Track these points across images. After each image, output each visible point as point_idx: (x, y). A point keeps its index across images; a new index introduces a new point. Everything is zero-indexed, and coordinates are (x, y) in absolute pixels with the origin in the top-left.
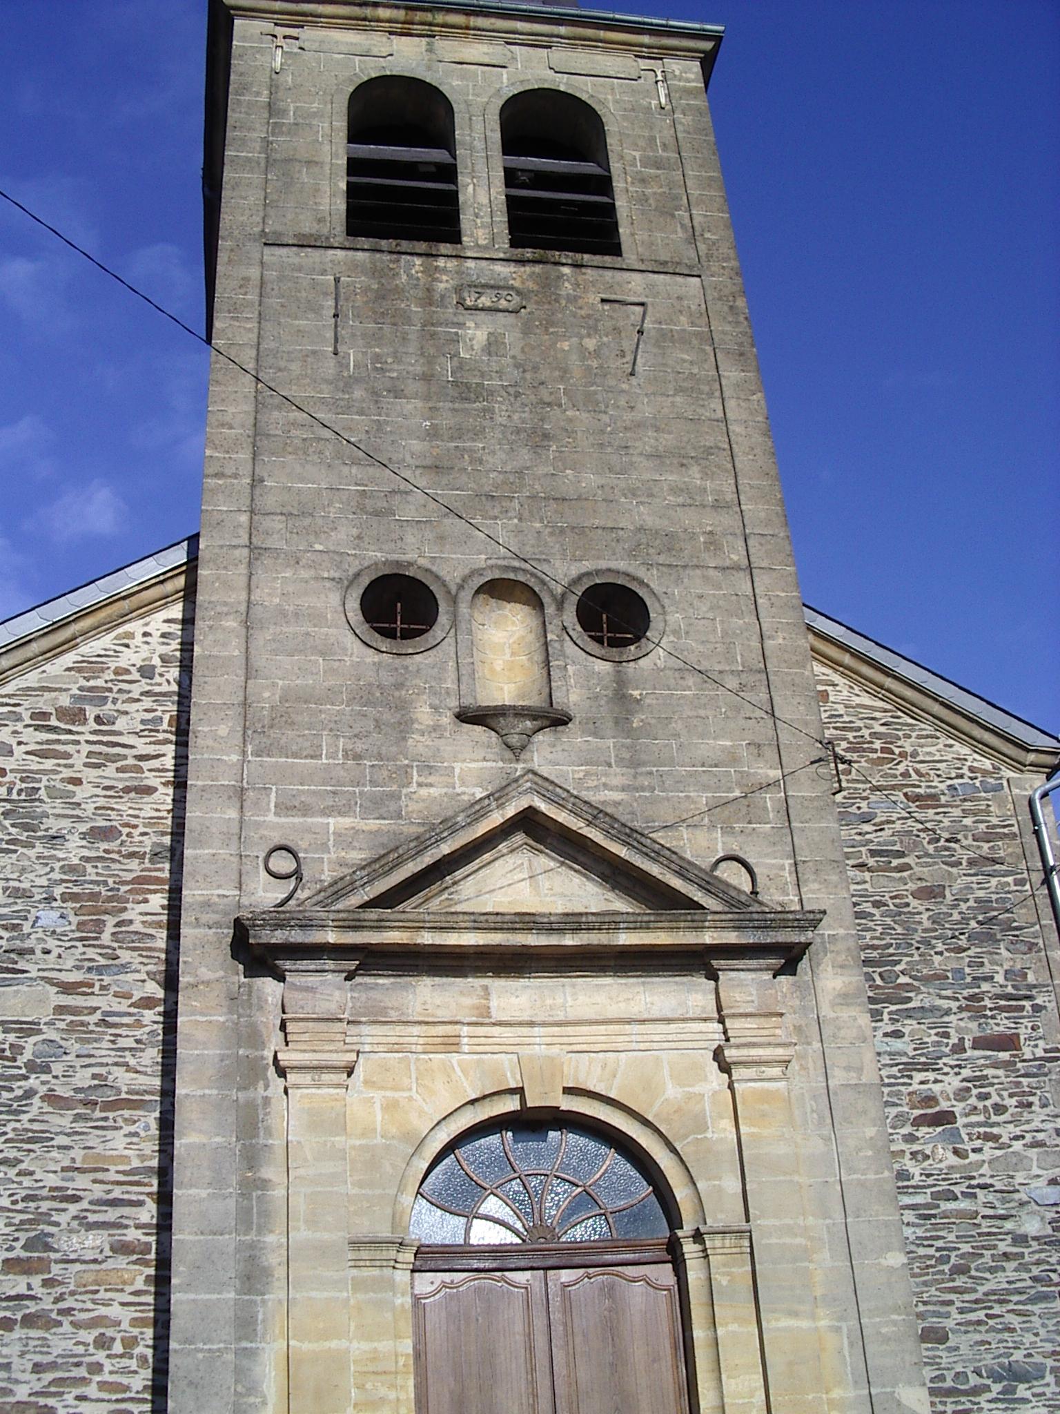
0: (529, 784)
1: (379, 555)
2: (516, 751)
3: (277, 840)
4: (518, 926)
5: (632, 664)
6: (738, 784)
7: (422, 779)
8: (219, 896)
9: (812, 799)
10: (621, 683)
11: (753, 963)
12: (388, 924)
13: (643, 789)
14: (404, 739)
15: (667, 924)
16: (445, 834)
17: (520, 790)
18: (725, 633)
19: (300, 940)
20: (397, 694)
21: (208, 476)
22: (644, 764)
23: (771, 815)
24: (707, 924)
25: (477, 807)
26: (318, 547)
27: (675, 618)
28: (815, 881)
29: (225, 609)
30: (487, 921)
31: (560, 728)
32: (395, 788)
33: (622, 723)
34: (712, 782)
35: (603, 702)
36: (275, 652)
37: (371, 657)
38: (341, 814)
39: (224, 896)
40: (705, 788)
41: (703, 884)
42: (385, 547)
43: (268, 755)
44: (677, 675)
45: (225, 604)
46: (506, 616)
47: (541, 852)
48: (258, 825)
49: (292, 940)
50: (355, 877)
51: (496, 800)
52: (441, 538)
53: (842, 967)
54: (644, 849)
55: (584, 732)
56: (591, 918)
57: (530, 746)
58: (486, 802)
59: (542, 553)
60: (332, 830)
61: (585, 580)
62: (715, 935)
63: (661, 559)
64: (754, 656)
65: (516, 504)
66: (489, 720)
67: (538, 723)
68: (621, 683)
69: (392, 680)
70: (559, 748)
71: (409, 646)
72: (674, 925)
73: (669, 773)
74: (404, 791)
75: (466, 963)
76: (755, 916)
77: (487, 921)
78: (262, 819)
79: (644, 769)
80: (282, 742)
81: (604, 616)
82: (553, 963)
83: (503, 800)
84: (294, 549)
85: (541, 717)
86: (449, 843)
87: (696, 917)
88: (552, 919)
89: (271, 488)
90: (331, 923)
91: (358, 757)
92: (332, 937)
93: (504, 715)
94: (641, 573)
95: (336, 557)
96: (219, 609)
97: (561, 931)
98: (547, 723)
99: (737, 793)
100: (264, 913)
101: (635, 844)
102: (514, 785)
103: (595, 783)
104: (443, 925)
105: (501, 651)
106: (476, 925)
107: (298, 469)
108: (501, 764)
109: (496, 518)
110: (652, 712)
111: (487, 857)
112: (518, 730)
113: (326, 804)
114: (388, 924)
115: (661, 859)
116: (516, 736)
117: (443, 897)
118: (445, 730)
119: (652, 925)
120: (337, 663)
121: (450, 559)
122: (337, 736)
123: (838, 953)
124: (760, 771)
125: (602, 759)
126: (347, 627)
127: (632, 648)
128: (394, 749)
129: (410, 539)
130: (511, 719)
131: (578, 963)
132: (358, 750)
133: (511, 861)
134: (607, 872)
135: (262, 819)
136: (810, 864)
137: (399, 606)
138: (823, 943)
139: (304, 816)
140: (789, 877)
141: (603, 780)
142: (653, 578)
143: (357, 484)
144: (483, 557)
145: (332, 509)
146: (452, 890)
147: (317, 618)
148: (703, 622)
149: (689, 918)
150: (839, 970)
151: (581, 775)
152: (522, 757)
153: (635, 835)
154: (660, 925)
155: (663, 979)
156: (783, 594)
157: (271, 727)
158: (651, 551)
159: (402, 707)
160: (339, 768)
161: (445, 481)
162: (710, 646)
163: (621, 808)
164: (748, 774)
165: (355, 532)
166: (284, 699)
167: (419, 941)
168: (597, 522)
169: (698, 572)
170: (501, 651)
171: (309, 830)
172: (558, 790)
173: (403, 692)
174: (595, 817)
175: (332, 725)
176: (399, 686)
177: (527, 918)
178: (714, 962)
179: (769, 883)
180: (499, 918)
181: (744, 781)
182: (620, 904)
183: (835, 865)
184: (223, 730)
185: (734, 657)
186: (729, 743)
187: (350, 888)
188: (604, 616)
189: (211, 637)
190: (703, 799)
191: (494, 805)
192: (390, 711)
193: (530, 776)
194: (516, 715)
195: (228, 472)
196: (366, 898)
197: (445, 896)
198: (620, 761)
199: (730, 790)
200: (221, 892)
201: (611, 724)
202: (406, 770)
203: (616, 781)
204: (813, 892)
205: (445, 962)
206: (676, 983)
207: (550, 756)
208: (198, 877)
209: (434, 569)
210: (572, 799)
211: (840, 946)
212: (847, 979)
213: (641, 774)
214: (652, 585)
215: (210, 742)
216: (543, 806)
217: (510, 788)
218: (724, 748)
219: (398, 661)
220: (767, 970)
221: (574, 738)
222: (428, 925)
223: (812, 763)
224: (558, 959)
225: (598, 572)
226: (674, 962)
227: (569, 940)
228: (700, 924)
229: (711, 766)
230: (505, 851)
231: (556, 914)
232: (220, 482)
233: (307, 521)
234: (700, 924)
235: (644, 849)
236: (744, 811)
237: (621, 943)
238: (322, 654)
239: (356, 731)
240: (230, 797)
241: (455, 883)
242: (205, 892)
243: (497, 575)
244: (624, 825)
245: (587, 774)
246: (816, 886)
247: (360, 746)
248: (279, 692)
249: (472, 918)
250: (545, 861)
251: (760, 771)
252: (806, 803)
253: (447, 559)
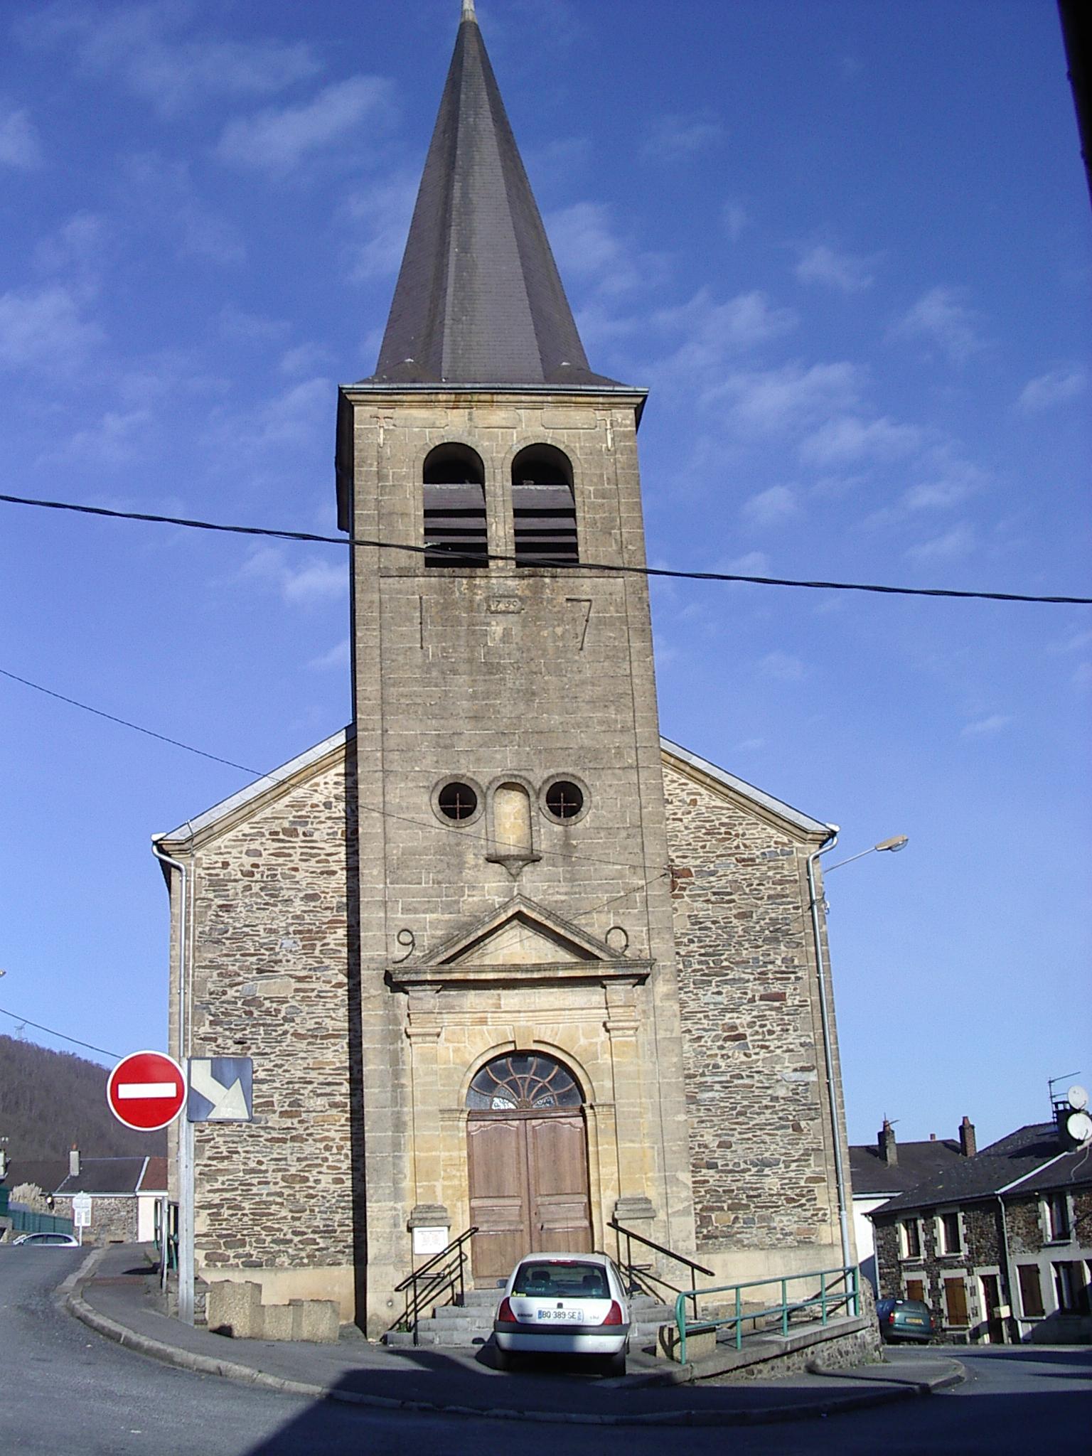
2: (515, 877)
3: (403, 927)
10: (567, 836)
33: (567, 857)
36: (398, 829)
40: (607, 892)
52: (478, 760)
63: (591, 765)
68: (567, 836)
71: (463, 822)
91: (439, 883)
92: (429, 977)
105: (508, 818)
121: (480, 773)
133: (512, 933)
137: (458, 801)
140: (645, 936)
142: (586, 777)
147: (417, 809)
159: (460, 855)
168: (558, 745)
170: (508, 818)
171: (417, 920)
176: (458, 844)
184: (375, 872)
192: (453, 859)
211: (668, 970)
216: (525, 910)
221: (543, 868)
233: (411, 754)
243: (507, 780)
247: (440, 877)
250: (527, 933)
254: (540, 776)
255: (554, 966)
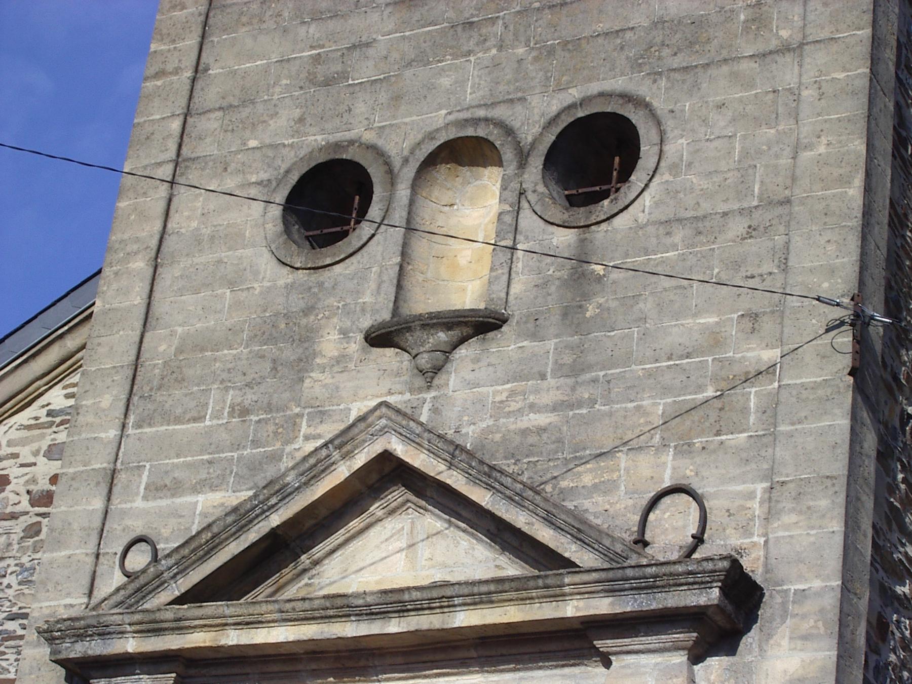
0: (383, 422)
1: (319, 138)
2: (431, 374)
3: (138, 532)
4: (331, 612)
5: (604, 226)
6: (715, 379)
7: (311, 431)
8: (65, 606)
9: (815, 386)
10: (581, 259)
11: (652, 641)
12: (187, 623)
13: (580, 404)
14: (301, 380)
15: (513, 595)
16: (273, 501)
17: (371, 430)
18: (745, 154)
19: (98, 652)
20: (304, 321)
21: (146, 79)
22: (590, 368)
23: (752, 419)
24: (567, 589)
25: (312, 461)
26: (253, 143)
27: (678, 146)
28: (793, 510)
29: (135, 247)
30: (294, 609)
31: (491, 335)
32: (278, 445)
33: (572, 315)
34: (677, 381)
35: (553, 289)
36: (181, 292)
37: (285, 277)
38: (213, 488)
39: (72, 606)
40: (666, 390)
41: (574, 532)
42: (329, 126)
43: (150, 425)
44: (662, 230)
45: (137, 240)
46: (485, 187)
47: (426, 510)
48: (124, 513)
49: (90, 652)
50: (161, 568)
51: (340, 447)
52: (397, 98)
53: (805, 638)
54: (508, 492)
55: (520, 336)
56: (416, 595)
57: (448, 365)
58: (324, 452)
59: (518, 89)
60: (199, 508)
61: (563, 117)
62: (581, 604)
63: (676, 62)
64: (780, 180)
65: (499, 28)
66: (396, 339)
67: (455, 334)
68: (581, 259)
69: (302, 304)
70: (484, 363)
71: (327, 255)
72: (524, 594)
73: (621, 377)
74: (288, 449)
75: (300, 667)
76: (630, 573)
77: (294, 609)
78: (128, 505)
79: (588, 376)
80: (167, 406)
81: (617, 159)
82: (400, 660)
83: (348, 447)
84: (224, 152)
85: (459, 324)
86: (280, 512)
87: (549, 581)
88: (369, 599)
89: (216, 76)
90: (129, 628)
91: (245, 412)
92: (131, 645)
93: (409, 329)
94: (643, 89)
95: (270, 153)
96: (129, 249)
97: (383, 615)
98: (466, 331)
99: (710, 392)
100: (58, 622)
101: (497, 485)
102: (362, 426)
103: (519, 405)
104: (248, 619)
105: (469, 238)
106: (284, 616)
107: (249, 42)
108: (408, 396)
109: (469, 53)
110: (615, 292)
111: (355, 524)
112: (427, 347)
113: (198, 477)
114: (187, 623)
115: (527, 503)
116: (425, 356)
117: (303, 582)
118: (351, 359)
119: (495, 597)
120: (245, 294)
121: (393, 129)
122: (227, 389)
123: (804, 617)
124: (749, 354)
125: (535, 370)
126: (535, 217)
127: (606, 202)
128: (286, 395)
129: (360, 108)
130: (418, 333)
131: (431, 657)
132: (246, 403)
133: (390, 525)
134: (493, 528)
135: (128, 505)
136: (792, 486)
137: (328, 202)
138: (784, 604)
139: (173, 496)
140: (756, 507)
141: (532, 398)
142: (658, 95)
143: (312, 47)
144: (444, 112)
145: (278, 89)
146: (314, 572)
147: (233, 238)
148: (716, 143)
149: (540, 582)
150: (799, 643)
151: (503, 397)
152: (436, 382)
153: (495, 474)
154: (505, 596)
155: (549, 672)
156: (841, 76)
157: (159, 389)
158: (666, 52)
159: (306, 339)
160: (222, 429)
161: (417, 16)
162: (717, 179)
163: (545, 436)
164: (731, 361)
165: (297, 113)
166: (180, 351)
167: (222, 643)
168: (600, 27)
169: (725, 69)
170: (469, 238)
171: (175, 513)
172: (412, 424)
173: (312, 318)
174: (453, 456)
175: (225, 375)
176: (308, 311)
177: (339, 602)
178: (595, 642)
179: (725, 520)
180: (307, 605)
181: (723, 374)
182: (511, 568)
183: (829, 483)
184: (106, 401)
185: (750, 189)
186: (712, 320)
187: (156, 583)
188: (617, 159)
189: (115, 286)
190: (657, 407)
191: (336, 455)
192: (288, 342)
193: (384, 410)
194: (424, 326)
195: (170, 67)
196: (177, 593)
197: (305, 580)
198: (560, 370)
199: (701, 388)
200: (68, 601)
201: (556, 318)
202: (294, 422)
203: (546, 399)
204: (787, 527)
205: (275, 668)
206: (563, 676)
207: (470, 376)
208: (50, 586)
209: (380, 143)
210: (426, 435)
211: (809, 606)
212: (807, 656)
213: (583, 383)
214: (655, 104)
215: (90, 418)
216: (400, 449)
217: (356, 430)
218: (705, 328)
219: (315, 277)
220: (677, 649)
221: (507, 345)
222: (230, 621)
223: (827, 331)
224: (404, 654)
225: (571, 107)
226: (553, 646)
227: (394, 626)
228: (557, 591)
229: (681, 357)
230: (380, 513)
231: (372, 593)
232: (159, 83)
233: (246, 112)
234: (557, 591)
235: (508, 492)
236: (713, 416)
237: (457, 625)
238: (232, 284)
239: (248, 379)
240: (98, 483)
241: (316, 563)
242: (52, 603)
243: (453, 134)
244: (482, 462)
245: (512, 393)
246: (793, 518)
247: (250, 397)
248: (176, 342)
249: (277, 606)
250: (432, 520)
251: (749, 354)
252: (805, 394)
253: (398, 126)
254: (537, 114)
255: (441, 596)
